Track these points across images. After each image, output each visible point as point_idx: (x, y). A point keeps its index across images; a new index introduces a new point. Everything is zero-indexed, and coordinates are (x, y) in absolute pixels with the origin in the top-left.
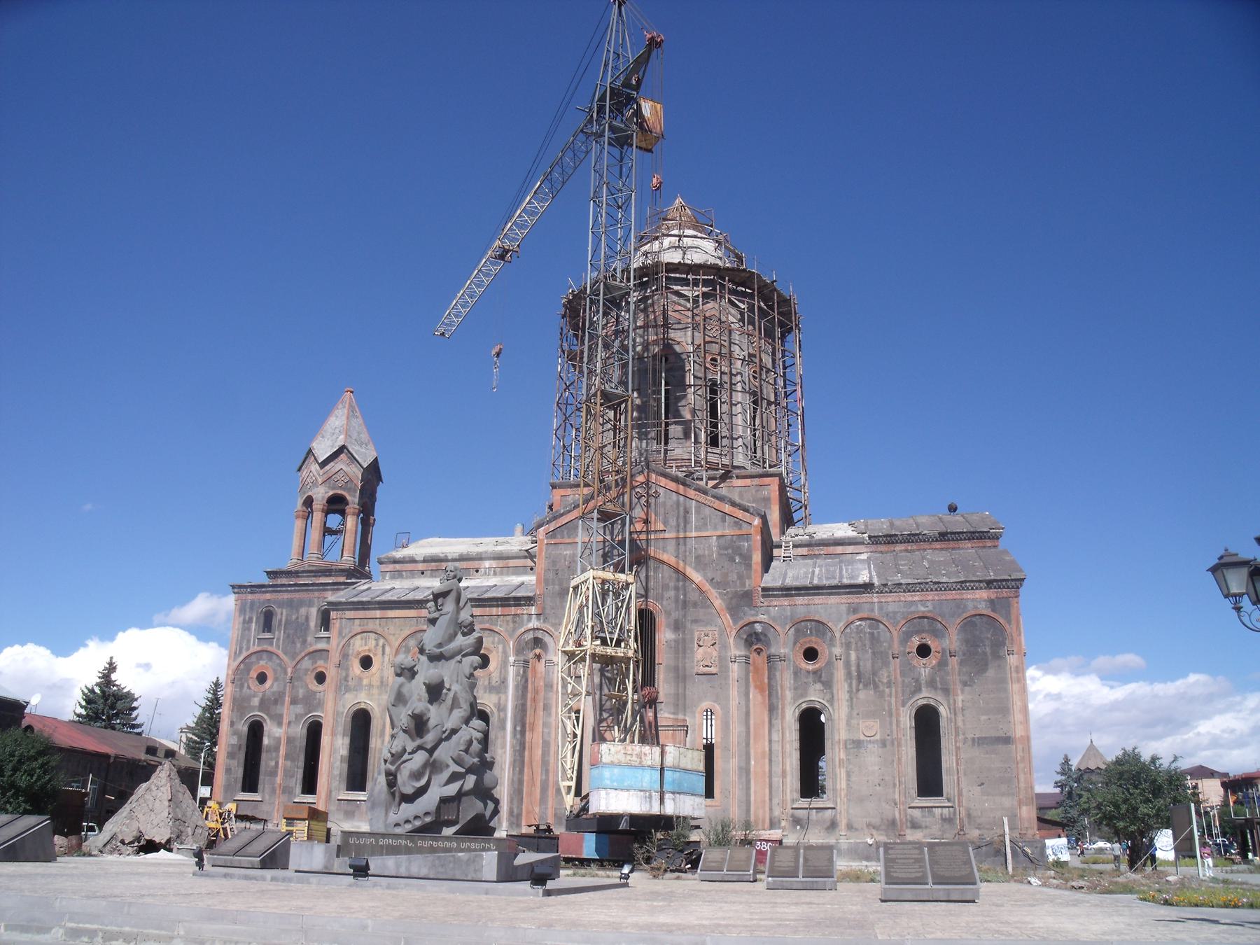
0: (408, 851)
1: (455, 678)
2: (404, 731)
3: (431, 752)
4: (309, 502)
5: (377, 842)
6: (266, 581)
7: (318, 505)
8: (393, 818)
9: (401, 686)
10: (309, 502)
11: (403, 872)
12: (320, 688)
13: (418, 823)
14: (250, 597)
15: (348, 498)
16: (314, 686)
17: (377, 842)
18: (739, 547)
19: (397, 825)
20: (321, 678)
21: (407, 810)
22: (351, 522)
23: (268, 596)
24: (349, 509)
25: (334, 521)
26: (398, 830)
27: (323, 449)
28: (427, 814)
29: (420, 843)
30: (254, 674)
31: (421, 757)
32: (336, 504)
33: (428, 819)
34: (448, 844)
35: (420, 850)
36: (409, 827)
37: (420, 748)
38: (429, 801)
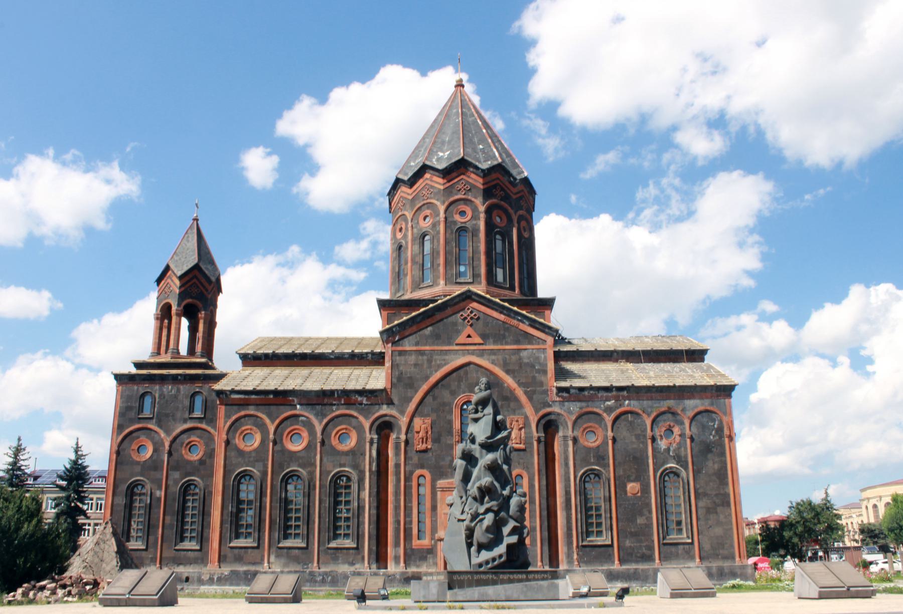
0: (494, 583)
5: (472, 577)
6: (134, 371)
17: (472, 577)
18: (538, 358)
21: (485, 555)
26: (482, 569)
29: (501, 576)
33: (503, 559)
35: (503, 582)
37: (488, 511)
38: (501, 549)
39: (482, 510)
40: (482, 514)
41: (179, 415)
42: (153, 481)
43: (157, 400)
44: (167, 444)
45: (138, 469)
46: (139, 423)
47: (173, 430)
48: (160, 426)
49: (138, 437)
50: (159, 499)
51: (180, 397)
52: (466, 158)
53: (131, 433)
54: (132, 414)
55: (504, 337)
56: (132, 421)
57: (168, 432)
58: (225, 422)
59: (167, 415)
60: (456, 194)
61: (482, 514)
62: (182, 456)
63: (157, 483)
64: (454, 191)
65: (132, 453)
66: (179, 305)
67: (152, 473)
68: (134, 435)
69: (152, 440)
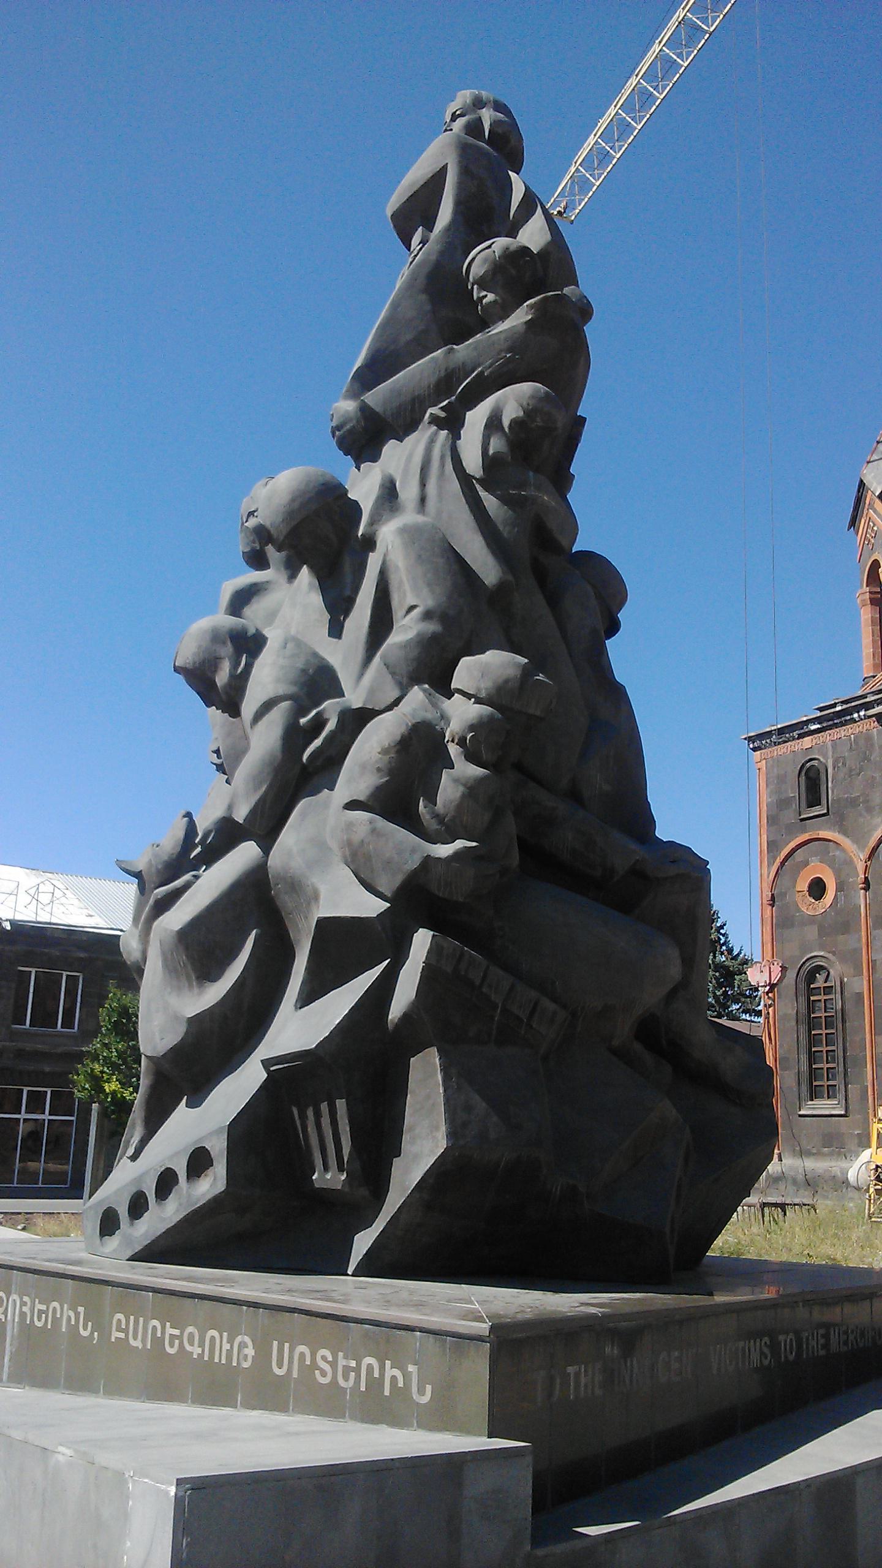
14: (782, 749)
23: (807, 742)
28: (199, 1161)
30: (803, 885)
33: (211, 1185)
42: (843, 959)
43: (830, 771)
44: (860, 867)
45: (812, 933)
46: (804, 831)
48: (844, 832)
49: (806, 863)
50: (860, 996)
53: (794, 851)
54: (790, 816)
56: (791, 831)
57: (859, 841)
59: (853, 802)
63: (852, 958)
65: (798, 898)
67: (841, 938)
68: (799, 855)
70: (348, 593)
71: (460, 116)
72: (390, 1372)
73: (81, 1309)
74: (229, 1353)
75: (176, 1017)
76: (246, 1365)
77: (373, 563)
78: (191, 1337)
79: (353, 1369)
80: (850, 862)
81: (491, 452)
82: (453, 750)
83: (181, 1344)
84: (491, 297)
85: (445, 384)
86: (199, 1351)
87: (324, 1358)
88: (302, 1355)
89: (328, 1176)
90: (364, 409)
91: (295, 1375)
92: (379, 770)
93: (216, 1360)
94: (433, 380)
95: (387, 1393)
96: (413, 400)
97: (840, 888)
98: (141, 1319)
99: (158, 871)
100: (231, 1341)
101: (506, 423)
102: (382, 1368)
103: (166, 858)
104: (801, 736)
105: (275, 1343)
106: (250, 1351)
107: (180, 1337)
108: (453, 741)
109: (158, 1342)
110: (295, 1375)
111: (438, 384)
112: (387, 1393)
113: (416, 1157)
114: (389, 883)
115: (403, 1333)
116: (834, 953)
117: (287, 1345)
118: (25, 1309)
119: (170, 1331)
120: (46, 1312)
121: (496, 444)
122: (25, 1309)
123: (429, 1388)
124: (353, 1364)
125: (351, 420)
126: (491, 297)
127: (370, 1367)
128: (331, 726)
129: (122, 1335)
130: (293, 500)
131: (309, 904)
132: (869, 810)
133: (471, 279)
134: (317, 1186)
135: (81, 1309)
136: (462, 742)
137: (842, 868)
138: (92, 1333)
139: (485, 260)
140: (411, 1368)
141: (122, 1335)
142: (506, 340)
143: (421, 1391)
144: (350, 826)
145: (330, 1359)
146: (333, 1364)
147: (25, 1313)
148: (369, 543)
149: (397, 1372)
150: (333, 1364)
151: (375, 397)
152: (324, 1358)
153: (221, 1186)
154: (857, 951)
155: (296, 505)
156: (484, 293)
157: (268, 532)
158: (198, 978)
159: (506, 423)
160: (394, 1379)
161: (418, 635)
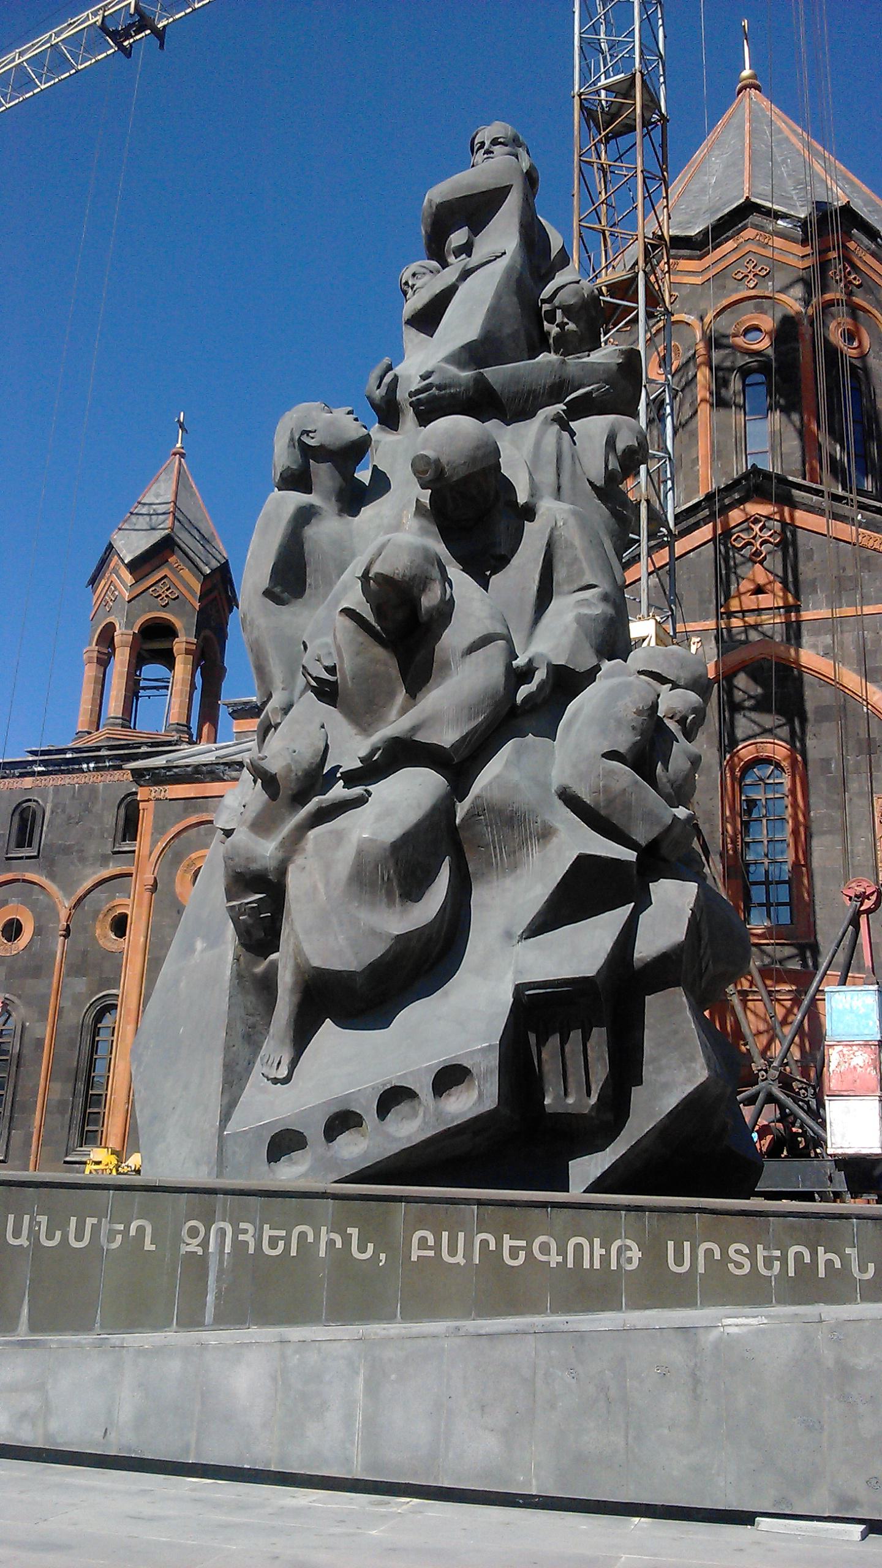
0: (355, 1296)
1: (547, 477)
2: (327, 691)
3: (459, 765)
4: (107, 637)
5: (168, 1237)
7: (123, 636)
8: (267, 1105)
9: (305, 516)
10: (107, 637)
11: (328, 1445)
12: (123, 943)
13: (407, 1130)
15: (178, 624)
16: (108, 940)
17: (168, 1237)
19: (284, 1143)
20: (120, 926)
21: (346, 1061)
22: (182, 667)
23: (28, 782)
24: (179, 645)
25: (152, 671)
26: (291, 1173)
27: (131, 544)
28: (449, 1078)
31: (410, 792)
32: (154, 642)
33: (463, 1105)
34: (593, 1253)
35: (426, 1293)
36: (354, 1150)
38: (464, 1018)
39: (351, 749)
40: (351, 778)
41: (92, 848)
42: (28, 1003)
44: (63, 914)
46: (9, 870)
47: (79, 882)
48: (52, 876)
50: (40, 1043)
51: (98, 808)
52: (753, 200)
55: (857, 583)
57: (67, 889)
58: (154, 843)
59: (66, 850)
60: (736, 291)
61: (351, 778)
62: (94, 939)
63: (39, 1005)
64: (731, 284)
66: (129, 625)
67: (30, 982)
69: (33, 906)
70: (503, 551)
71: (501, 143)
72: (822, 1256)
73: (354, 1232)
74: (605, 1259)
75: (374, 933)
76: (629, 1267)
77: (534, 536)
78: (545, 1249)
79: (777, 1258)
80: (53, 909)
81: (610, 468)
82: (672, 725)
83: (530, 1254)
84: (571, 326)
85: (557, 391)
86: (560, 1259)
87: (738, 1252)
88: (709, 1252)
89: (570, 1101)
90: (480, 381)
91: (701, 1269)
92: (634, 728)
93: (586, 1265)
94: (549, 381)
95: (822, 1273)
96: (529, 392)
97: (38, 931)
98: (461, 1235)
99: (298, 779)
100: (606, 1245)
101: (620, 446)
102: (814, 1254)
103: (305, 766)
104: (22, 775)
105: (671, 1244)
106: (636, 1254)
107: (529, 1250)
108: (671, 718)
109: (491, 1258)
110: (701, 1269)
111: (553, 386)
112: (822, 1273)
113: (666, 1087)
114: (643, 835)
115: (837, 1221)
116: (19, 997)
117: (687, 1245)
118: (241, 1237)
119: (507, 1242)
120: (287, 1240)
121: (614, 464)
122: (241, 1237)
123: (871, 1266)
124: (778, 1253)
125: (460, 386)
126: (571, 326)
127: (799, 1256)
128: (540, 675)
129: (431, 1253)
130: (478, 448)
131: (523, 843)
132: (82, 860)
133: (556, 302)
134: (548, 1110)
135: (354, 1232)
136: (682, 721)
137: (44, 913)
138: (376, 1254)
139: (576, 293)
140: (848, 1251)
141: (431, 1253)
142: (604, 371)
143: (863, 1269)
144: (610, 773)
145: (747, 1251)
146: (752, 1257)
147: (246, 1243)
148: (529, 512)
149: (831, 1256)
150: (752, 1257)
151: (495, 374)
152: (738, 1252)
153: (491, 1102)
154: (45, 998)
155: (480, 453)
156: (566, 320)
157: (443, 470)
158: (400, 896)
159: (620, 446)
160: (829, 1263)
161: (603, 613)
